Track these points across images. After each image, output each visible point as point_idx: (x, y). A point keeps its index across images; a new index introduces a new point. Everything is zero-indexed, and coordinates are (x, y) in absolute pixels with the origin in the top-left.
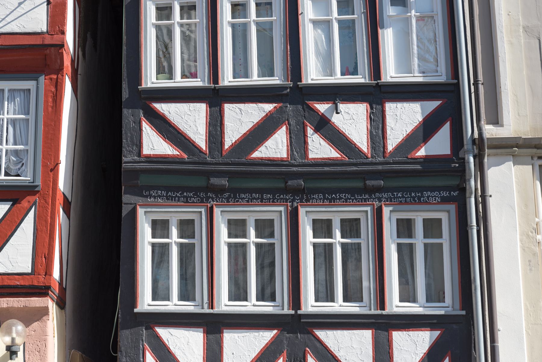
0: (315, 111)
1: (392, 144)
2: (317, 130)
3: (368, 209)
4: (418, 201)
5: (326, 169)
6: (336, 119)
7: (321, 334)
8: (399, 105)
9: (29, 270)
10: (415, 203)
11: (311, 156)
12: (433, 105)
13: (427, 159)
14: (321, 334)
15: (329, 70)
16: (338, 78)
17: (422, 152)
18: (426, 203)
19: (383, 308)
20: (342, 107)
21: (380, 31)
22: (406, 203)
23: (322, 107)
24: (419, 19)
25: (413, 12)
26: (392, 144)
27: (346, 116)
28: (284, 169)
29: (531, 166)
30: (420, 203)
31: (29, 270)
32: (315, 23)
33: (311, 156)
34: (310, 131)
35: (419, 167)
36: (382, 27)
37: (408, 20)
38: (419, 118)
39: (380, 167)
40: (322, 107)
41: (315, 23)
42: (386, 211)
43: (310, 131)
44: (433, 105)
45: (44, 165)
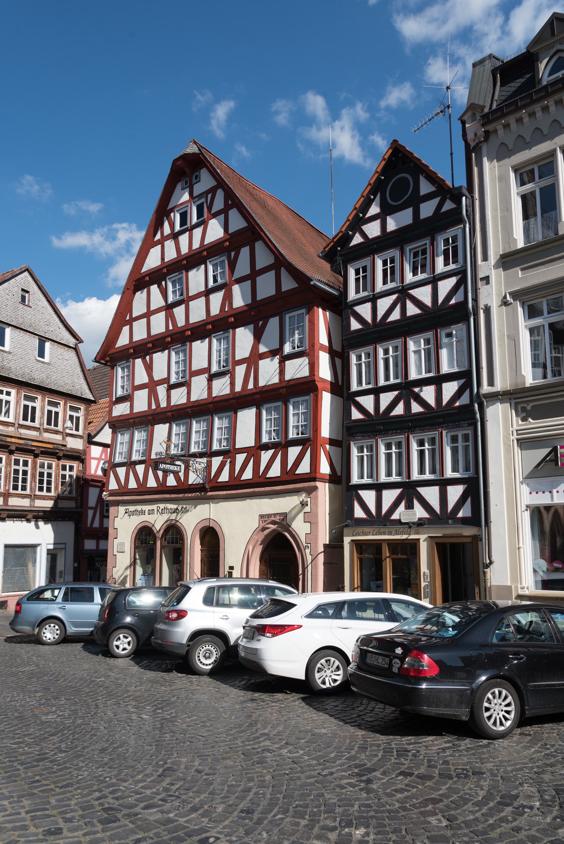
0: (414, 392)
1: (444, 403)
2: (414, 401)
3: (437, 432)
4: (458, 427)
5: (416, 417)
6: (422, 395)
7: (420, 489)
8: (448, 383)
9: (309, 472)
10: (457, 427)
11: (413, 412)
12: (463, 381)
13: (460, 407)
14: (420, 489)
15: (420, 372)
16: (424, 375)
17: (457, 404)
18: (462, 427)
19: (443, 476)
20: (424, 388)
21: (440, 350)
22: (453, 428)
23: (416, 390)
24: (457, 342)
25: (454, 339)
26: (444, 403)
27: (426, 392)
28: (402, 419)
29: (509, 404)
30: (459, 427)
31: (309, 472)
32: (415, 352)
33: (413, 412)
34: (412, 401)
35: (456, 411)
36: (441, 348)
37: (453, 342)
38: (457, 388)
39: (440, 413)
40: (416, 390)
41: (415, 352)
42: (444, 433)
43: (412, 401)
44: (463, 381)
45: (313, 429)
